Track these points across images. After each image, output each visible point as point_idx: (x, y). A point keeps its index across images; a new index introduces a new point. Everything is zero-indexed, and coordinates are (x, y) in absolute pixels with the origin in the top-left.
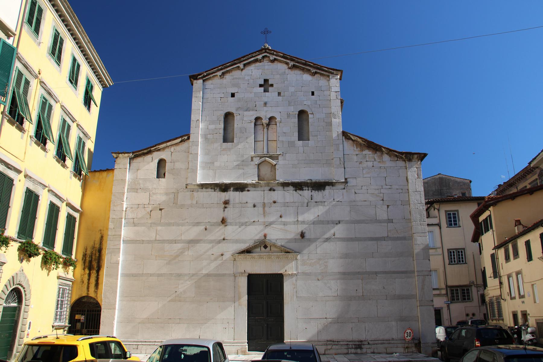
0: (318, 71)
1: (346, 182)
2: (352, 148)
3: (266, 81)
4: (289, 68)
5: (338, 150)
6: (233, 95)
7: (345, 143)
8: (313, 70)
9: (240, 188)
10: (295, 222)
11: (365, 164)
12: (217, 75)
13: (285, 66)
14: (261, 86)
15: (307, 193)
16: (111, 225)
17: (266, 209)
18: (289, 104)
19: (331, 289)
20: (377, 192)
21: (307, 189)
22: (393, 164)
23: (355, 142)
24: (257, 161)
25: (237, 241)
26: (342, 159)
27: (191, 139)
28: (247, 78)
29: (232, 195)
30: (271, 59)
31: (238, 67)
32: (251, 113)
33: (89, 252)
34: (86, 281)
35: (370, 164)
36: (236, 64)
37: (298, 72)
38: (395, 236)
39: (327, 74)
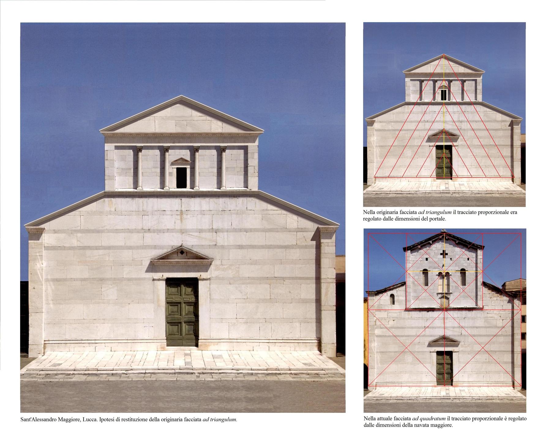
5: (253, 158)
10: (209, 230)
19: (241, 293)
38: (303, 244)
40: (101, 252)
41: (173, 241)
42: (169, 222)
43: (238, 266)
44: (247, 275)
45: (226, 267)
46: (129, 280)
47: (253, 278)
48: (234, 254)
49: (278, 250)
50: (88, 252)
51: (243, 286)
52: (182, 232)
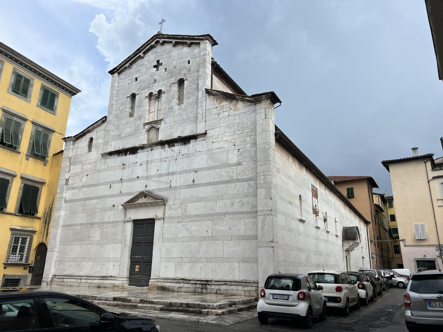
0: (192, 41)
1: (205, 134)
2: (213, 103)
3: (158, 61)
4: (174, 46)
6: (136, 79)
7: (208, 99)
8: (189, 42)
9: (133, 151)
10: (166, 174)
11: (221, 116)
12: (126, 67)
13: (171, 46)
14: (155, 66)
15: (177, 148)
16: (58, 191)
17: (149, 165)
18: (172, 77)
19: (188, 231)
20: (230, 138)
21: (177, 144)
22: (247, 109)
23: (216, 97)
24: (147, 127)
25: (128, 194)
26: (204, 115)
27: (107, 120)
28: (146, 63)
29: (130, 158)
30: (161, 42)
31: (140, 56)
32: (146, 91)
33: (47, 211)
34: (43, 232)
35: (226, 114)
36: (137, 54)
37: (179, 47)
39: (198, 41)
40: (95, 201)
41: (138, 187)
42: (140, 171)
43: (186, 205)
44: (193, 213)
45: (176, 206)
46: (109, 223)
47: (199, 216)
48: (185, 193)
49: (220, 186)
50: (88, 202)
51: (189, 224)
52: (147, 178)
